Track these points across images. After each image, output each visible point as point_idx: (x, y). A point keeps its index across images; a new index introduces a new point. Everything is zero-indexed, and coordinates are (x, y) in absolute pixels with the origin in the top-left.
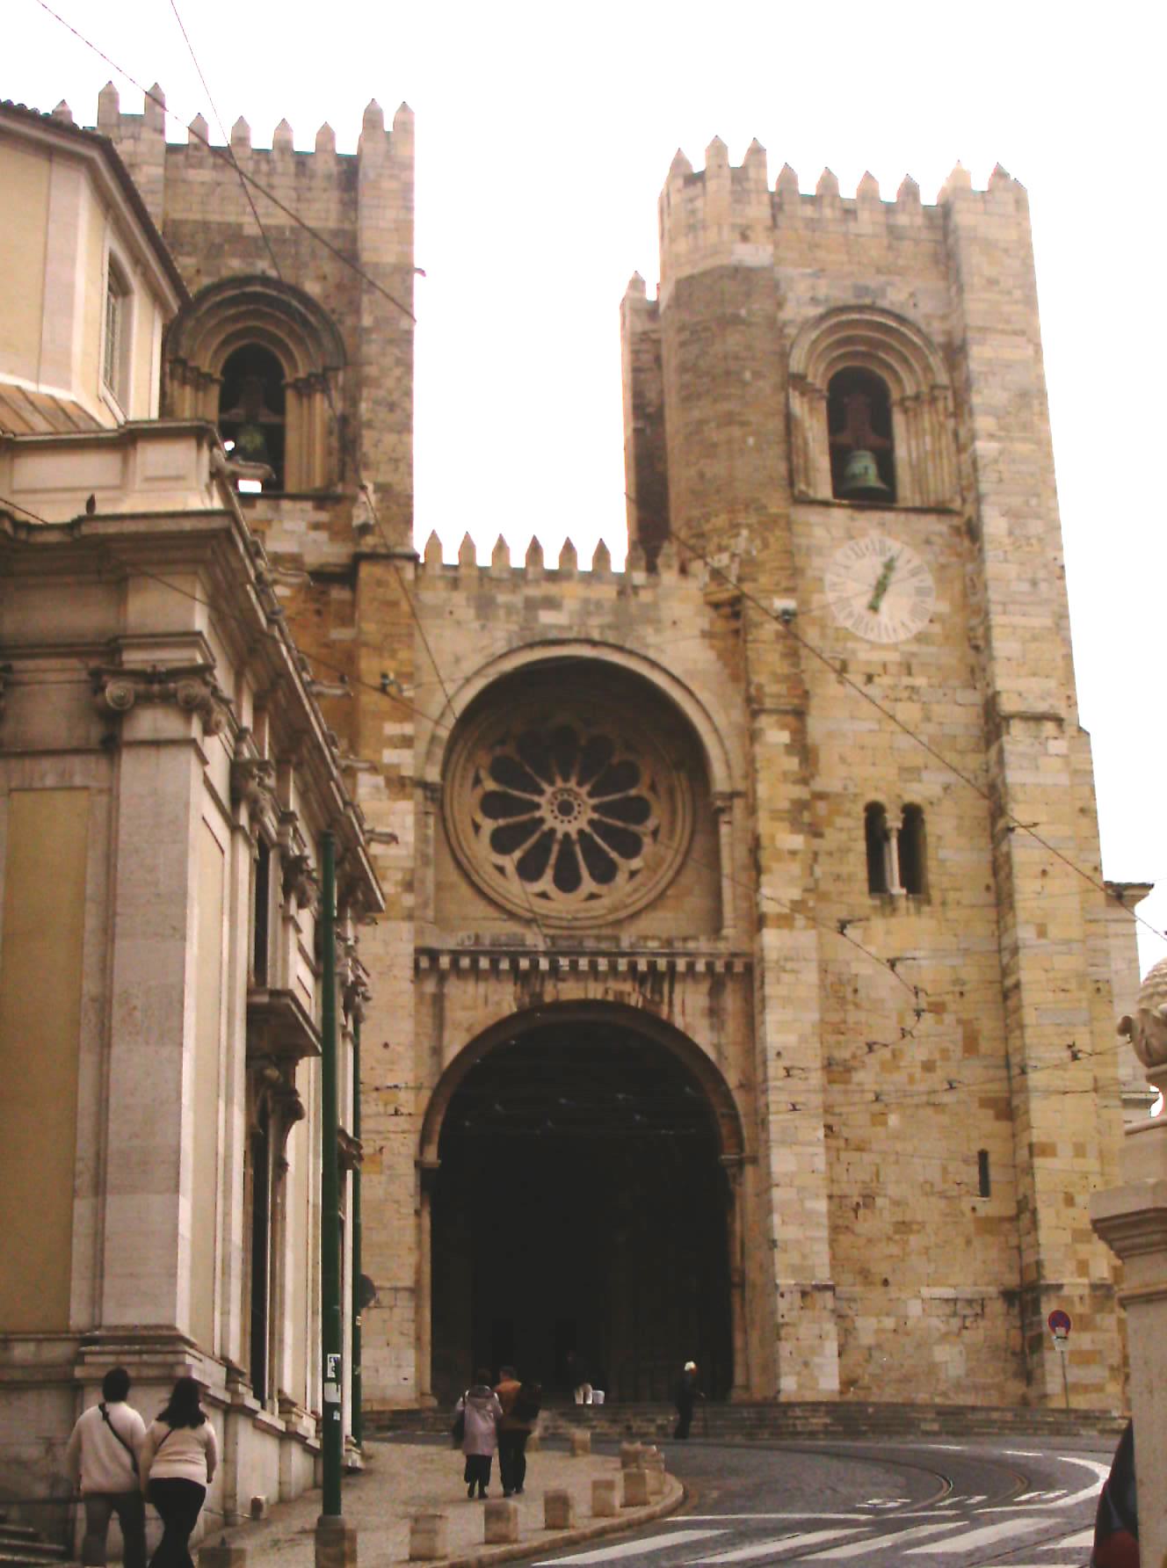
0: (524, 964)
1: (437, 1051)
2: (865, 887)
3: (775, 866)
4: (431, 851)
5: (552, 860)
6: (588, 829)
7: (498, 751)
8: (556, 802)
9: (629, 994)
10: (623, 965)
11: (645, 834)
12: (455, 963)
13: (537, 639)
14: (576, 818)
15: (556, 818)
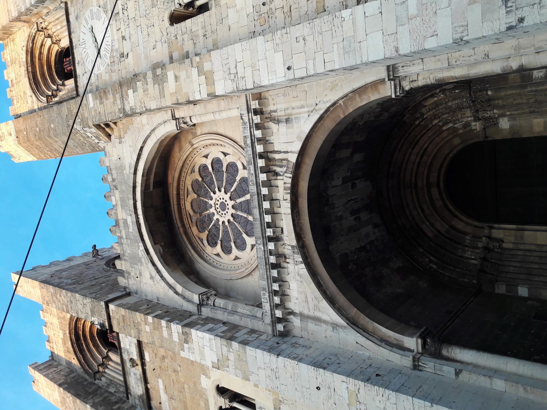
0: (273, 259)
1: (335, 326)
2: (207, 13)
3: (184, 91)
4: (230, 305)
5: (245, 215)
6: (229, 194)
7: (205, 242)
8: (221, 212)
9: (285, 183)
10: (265, 191)
11: (226, 160)
12: (277, 306)
13: (138, 234)
14: (226, 201)
15: (227, 212)
